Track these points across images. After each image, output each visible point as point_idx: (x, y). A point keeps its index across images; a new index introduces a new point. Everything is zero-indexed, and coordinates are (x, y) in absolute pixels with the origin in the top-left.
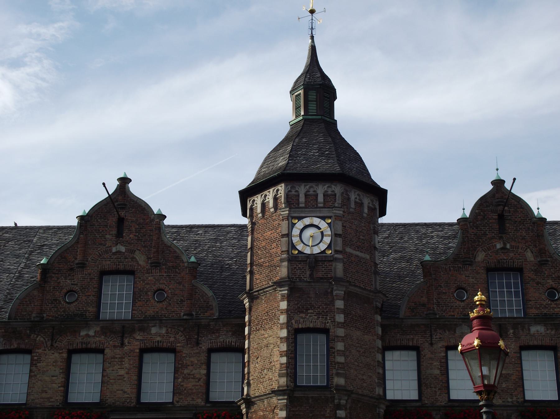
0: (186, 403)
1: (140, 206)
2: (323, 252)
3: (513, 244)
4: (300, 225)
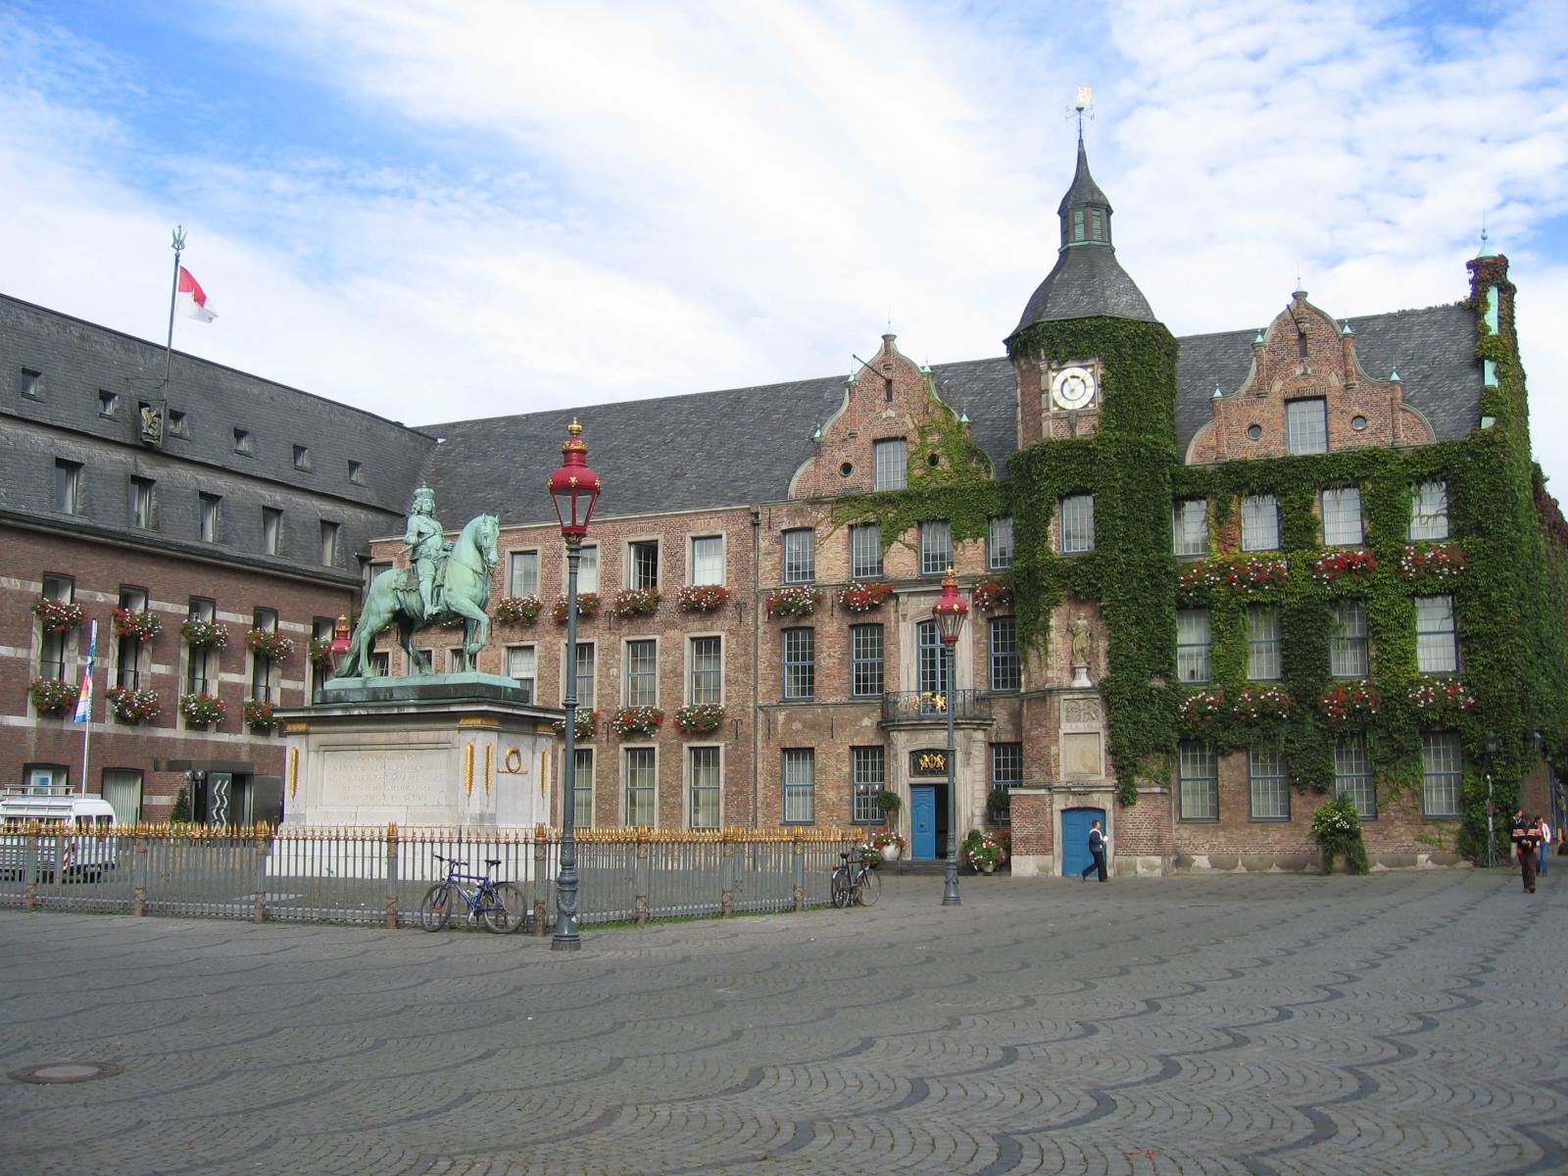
0: (966, 572)
1: (906, 365)
2: (1086, 406)
3: (1315, 367)
4: (1061, 377)
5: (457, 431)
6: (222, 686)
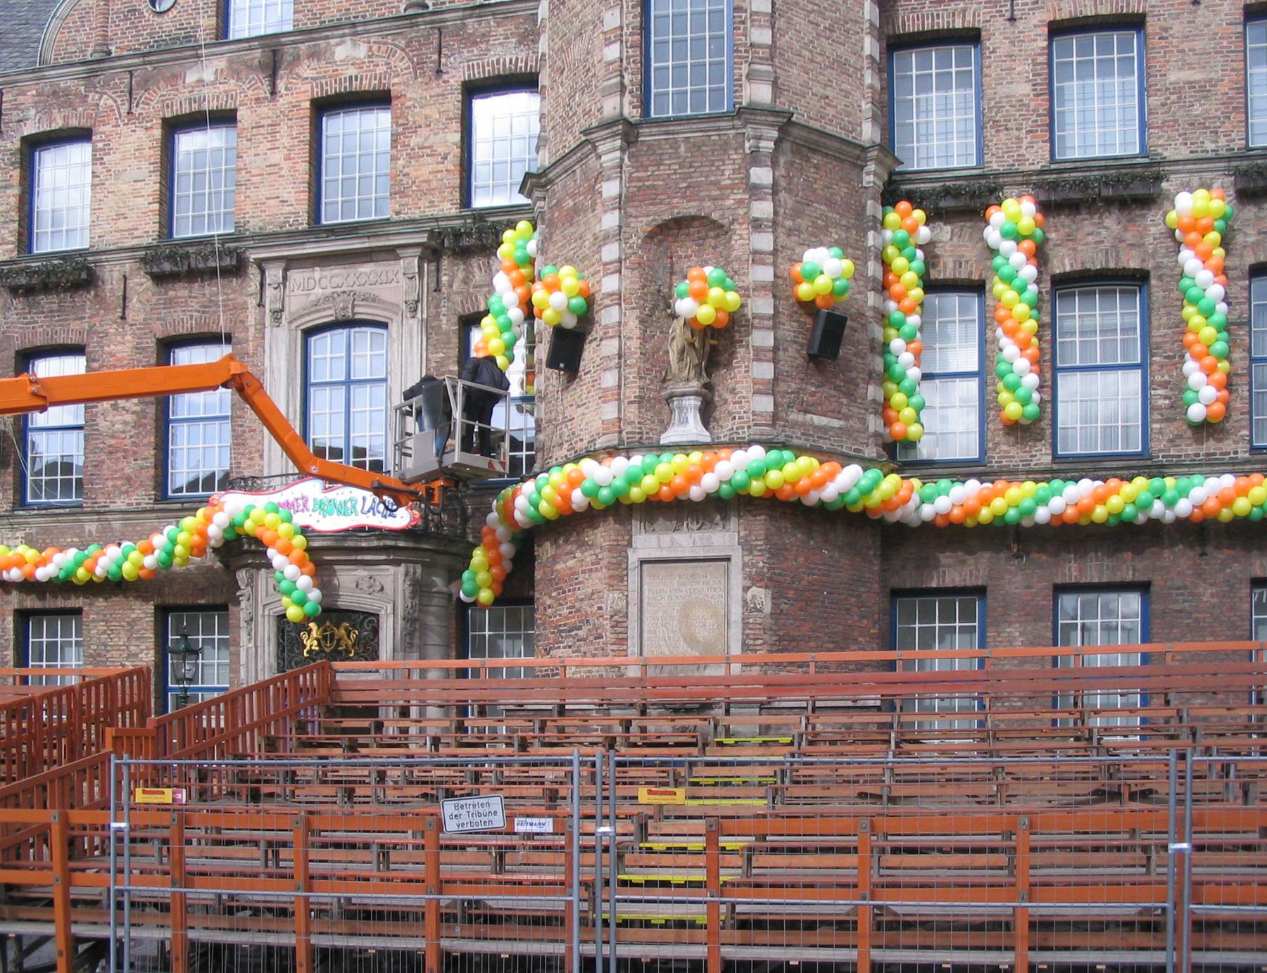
0: (416, 214)
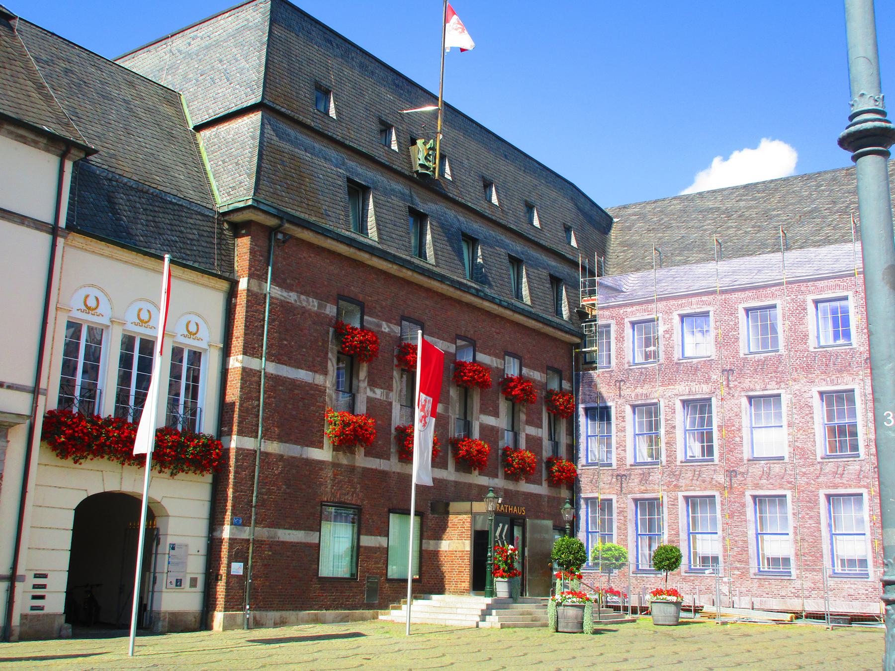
5: (630, 211)
6: (483, 427)
